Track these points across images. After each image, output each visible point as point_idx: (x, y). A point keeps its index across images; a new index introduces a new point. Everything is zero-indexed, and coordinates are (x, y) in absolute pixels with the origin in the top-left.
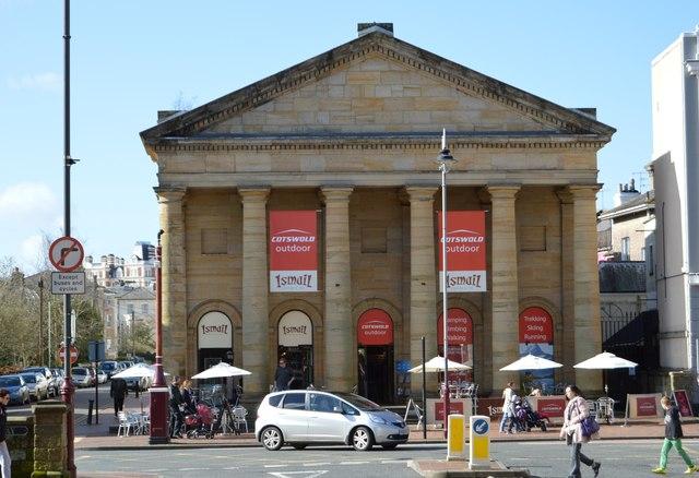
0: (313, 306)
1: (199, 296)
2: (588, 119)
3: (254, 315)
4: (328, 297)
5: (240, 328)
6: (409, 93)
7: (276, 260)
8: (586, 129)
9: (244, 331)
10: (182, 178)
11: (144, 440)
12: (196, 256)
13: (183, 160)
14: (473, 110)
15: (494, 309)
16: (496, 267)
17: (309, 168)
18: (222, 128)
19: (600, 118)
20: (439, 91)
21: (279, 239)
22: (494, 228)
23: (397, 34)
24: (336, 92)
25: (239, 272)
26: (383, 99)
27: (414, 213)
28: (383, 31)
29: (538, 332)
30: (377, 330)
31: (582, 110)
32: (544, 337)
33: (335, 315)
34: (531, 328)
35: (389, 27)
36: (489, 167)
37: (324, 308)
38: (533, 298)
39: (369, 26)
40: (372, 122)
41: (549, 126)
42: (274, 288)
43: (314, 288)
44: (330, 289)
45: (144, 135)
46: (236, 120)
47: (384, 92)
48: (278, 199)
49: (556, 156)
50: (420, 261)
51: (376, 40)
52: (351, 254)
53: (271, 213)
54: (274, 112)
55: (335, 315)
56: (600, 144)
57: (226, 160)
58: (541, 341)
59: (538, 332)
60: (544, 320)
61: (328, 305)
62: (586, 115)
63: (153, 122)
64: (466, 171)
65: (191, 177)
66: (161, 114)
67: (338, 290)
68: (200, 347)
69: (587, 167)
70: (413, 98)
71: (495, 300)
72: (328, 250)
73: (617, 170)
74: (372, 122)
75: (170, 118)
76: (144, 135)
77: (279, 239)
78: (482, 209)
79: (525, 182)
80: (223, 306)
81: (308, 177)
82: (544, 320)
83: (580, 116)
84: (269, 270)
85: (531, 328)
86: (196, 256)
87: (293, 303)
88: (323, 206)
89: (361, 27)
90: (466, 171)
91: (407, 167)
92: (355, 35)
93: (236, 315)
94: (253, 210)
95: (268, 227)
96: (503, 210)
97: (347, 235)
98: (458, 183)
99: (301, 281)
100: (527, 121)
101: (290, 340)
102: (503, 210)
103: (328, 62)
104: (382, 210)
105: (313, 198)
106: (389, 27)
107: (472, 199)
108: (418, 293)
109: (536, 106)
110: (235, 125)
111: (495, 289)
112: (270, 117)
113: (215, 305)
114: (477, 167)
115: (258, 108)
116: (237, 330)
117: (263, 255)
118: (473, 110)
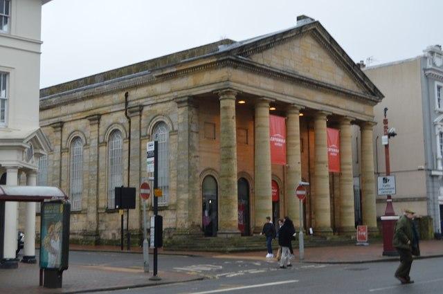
10: (239, 85)
17: (288, 93)
20: (329, 63)
24: (296, 50)
26: (312, 60)
36: (344, 107)
47: (312, 56)
51: (312, 31)
64: (338, 107)
65: (243, 86)
69: (370, 113)
81: (288, 97)
90: (338, 107)
110: (259, 59)
112: (272, 59)
118: (337, 78)
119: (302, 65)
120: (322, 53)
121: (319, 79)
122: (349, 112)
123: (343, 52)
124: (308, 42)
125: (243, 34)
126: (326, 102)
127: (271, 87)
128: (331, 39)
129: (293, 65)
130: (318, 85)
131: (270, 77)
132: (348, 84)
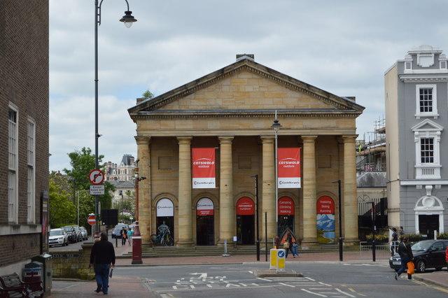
0: (213, 195)
1: (156, 191)
2: (351, 103)
3: (184, 200)
4: (221, 191)
5: (177, 207)
6: (262, 89)
7: (194, 172)
8: (350, 109)
9: (179, 208)
10: (149, 132)
11: (129, 261)
12: (155, 170)
13: (149, 124)
14: (292, 100)
15: (304, 197)
16: (305, 177)
18: (169, 107)
19: (358, 102)
20: (276, 89)
21: (197, 163)
22: (305, 157)
23: (256, 60)
24: (225, 89)
25: (177, 178)
26: (248, 92)
27: (264, 149)
28: (249, 58)
29: (326, 209)
30: (246, 207)
31: (349, 98)
32: (330, 211)
33: (225, 200)
34: (323, 206)
35: (252, 56)
36: (301, 126)
37: (219, 197)
38: (327, 192)
39: (242, 56)
40: (243, 103)
41: (332, 107)
42: (194, 187)
43: (213, 186)
44: (223, 189)
45: (130, 111)
46: (176, 103)
47: (249, 89)
48: (198, 142)
49: (335, 120)
50: (267, 173)
51: (245, 65)
52: (233, 169)
53: (194, 150)
54: (194, 99)
55: (225, 200)
56: (358, 115)
57: (170, 124)
58: (329, 213)
59: (326, 209)
60: (330, 202)
61: (221, 195)
62: (349, 100)
63: (134, 104)
64: (290, 129)
66: (138, 100)
67: (225, 188)
68: (159, 215)
69: (351, 126)
70: (264, 92)
71: (305, 193)
72: (221, 167)
73: (365, 128)
74: (243, 103)
75: (143, 102)
76: (130, 111)
77: (197, 163)
78: (299, 147)
79: (319, 134)
80: (169, 196)
81: (212, 132)
82: (330, 202)
83: (347, 101)
84: (192, 177)
85: (323, 206)
86: (155, 170)
87: (205, 193)
88: (219, 145)
89: (238, 56)
91: (263, 127)
92: (234, 60)
93: (174, 198)
94: (184, 149)
95: (191, 156)
96: (309, 148)
97: (231, 160)
98: (238, 135)
99: (207, 183)
100: (321, 105)
101: (162, 213)
102: (309, 148)
103: (223, 74)
104: (247, 148)
105: (212, 142)
106: (252, 56)
107: (291, 143)
108: (266, 189)
109: (325, 96)
110: (174, 106)
111: (305, 187)
112: (194, 103)
113: (164, 195)
114: (296, 127)
115: (187, 97)
116: (176, 208)
117: (189, 170)
118: (292, 100)
119: (233, 99)
120: (265, 82)
121: (261, 107)
122: (309, 131)
123: (290, 78)
124: (245, 76)
125: (158, 91)
126: (267, 127)
127: (191, 127)
128: (269, 70)
129: (221, 104)
130: (252, 115)
131: (186, 119)
132: (309, 103)
